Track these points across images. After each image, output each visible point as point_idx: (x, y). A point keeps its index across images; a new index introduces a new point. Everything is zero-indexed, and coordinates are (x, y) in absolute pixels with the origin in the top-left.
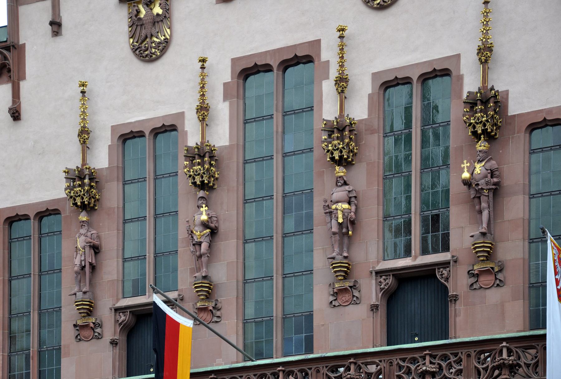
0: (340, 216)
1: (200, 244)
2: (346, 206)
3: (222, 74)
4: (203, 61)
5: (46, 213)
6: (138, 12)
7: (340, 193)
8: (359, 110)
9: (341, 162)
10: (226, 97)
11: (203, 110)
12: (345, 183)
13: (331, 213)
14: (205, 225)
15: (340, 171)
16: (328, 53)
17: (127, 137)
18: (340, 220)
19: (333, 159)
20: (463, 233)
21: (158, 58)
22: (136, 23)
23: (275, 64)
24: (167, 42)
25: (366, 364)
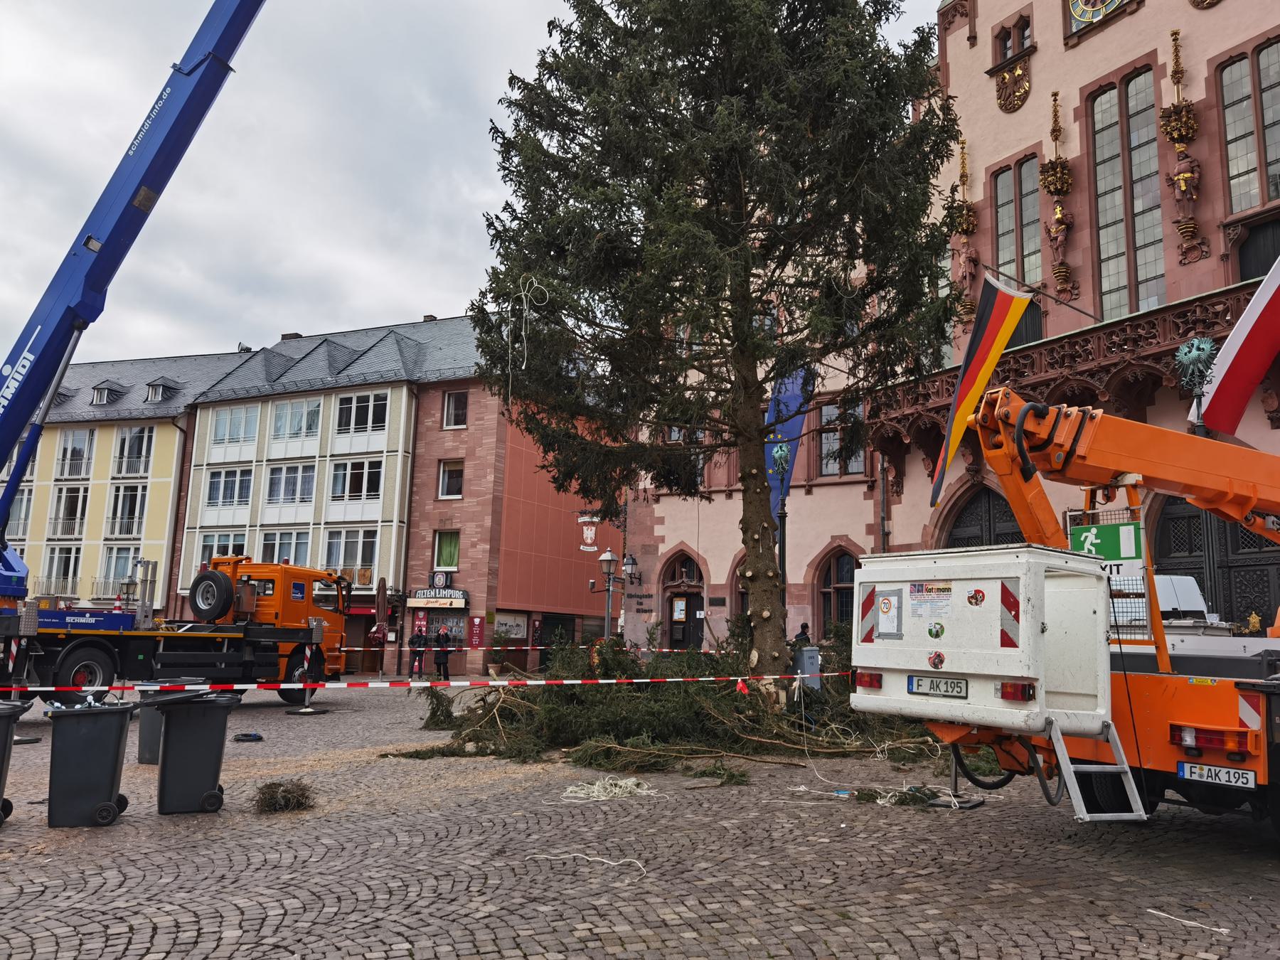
0: (1182, 184)
1: (1056, 239)
2: (1188, 175)
3: (1072, 100)
4: (1055, 94)
6: (1004, 78)
8: (1197, 93)
9: (1181, 139)
11: (1057, 133)
12: (1187, 156)
13: (1172, 183)
14: (1059, 222)
15: (1179, 147)
16: (1165, 58)
18: (1183, 188)
19: (1173, 139)
21: (1020, 107)
22: (1001, 88)
23: (1116, 80)
24: (1027, 93)
25: (1213, 305)
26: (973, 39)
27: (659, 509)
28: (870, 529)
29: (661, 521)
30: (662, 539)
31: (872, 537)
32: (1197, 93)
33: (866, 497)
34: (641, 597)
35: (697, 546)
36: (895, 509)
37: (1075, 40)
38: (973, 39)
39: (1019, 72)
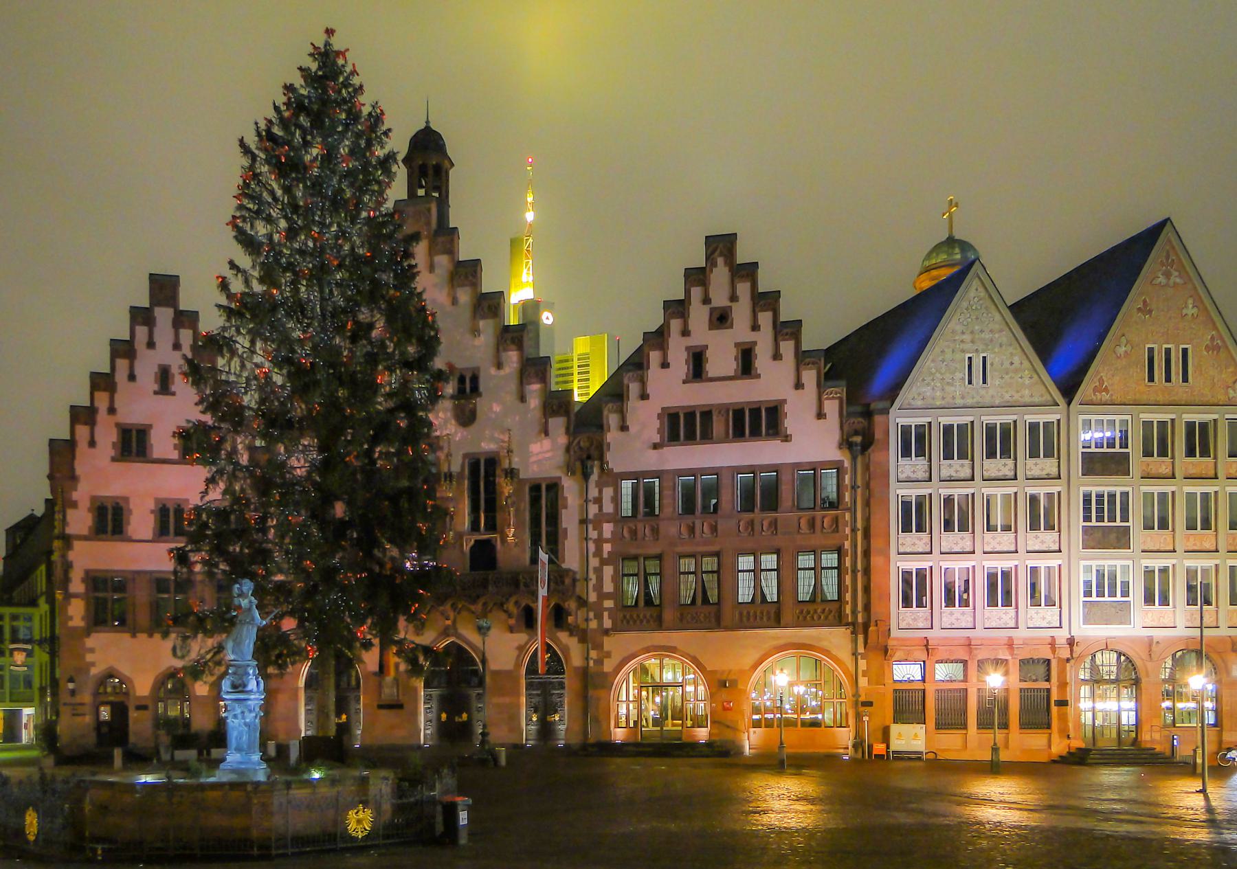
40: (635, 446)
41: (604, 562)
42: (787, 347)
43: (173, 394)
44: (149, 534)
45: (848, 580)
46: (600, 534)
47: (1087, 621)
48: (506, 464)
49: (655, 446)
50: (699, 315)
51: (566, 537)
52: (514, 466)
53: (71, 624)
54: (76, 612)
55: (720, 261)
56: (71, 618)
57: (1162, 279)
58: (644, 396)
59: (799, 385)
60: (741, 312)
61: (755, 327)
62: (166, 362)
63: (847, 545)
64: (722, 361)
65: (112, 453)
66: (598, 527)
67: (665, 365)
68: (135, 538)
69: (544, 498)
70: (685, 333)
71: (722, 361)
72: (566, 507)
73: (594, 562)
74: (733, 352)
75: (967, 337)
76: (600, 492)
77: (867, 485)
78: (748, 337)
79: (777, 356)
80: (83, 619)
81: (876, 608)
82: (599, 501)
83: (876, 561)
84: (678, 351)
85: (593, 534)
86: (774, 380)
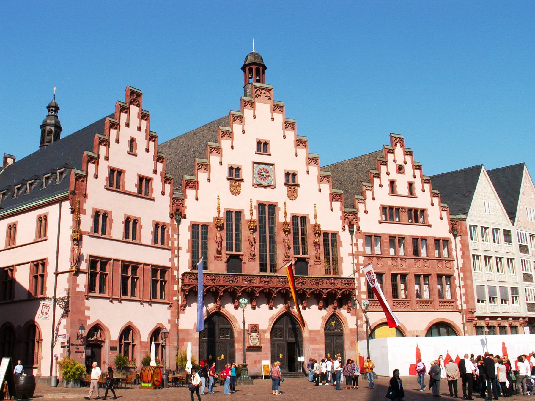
3: (255, 204)
5: (205, 226)
7: (286, 238)
10: (255, 209)
11: (251, 211)
17: (229, 213)
20: (312, 252)
26: (221, 164)
27: (88, 303)
28: (169, 321)
29: (88, 308)
30: (89, 318)
31: (170, 325)
32: (289, 220)
33: (169, 309)
34: (78, 345)
35: (105, 322)
36: (181, 315)
37: (256, 186)
38: (221, 164)
39: (237, 184)
40: (370, 221)
41: (361, 276)
42: (427, 186)
43: (136, 155)
44: (121, 237)
45: (457, 290)
46: (358, 261)
47: (529, 311)
48: (312, 221)
49: (380, 223)
50: (392, 167)
51: (343, 262)
52: (318, 223)
53: (78, 289)
54: (82, 280)
55: (399, 145)
56: (78, 286)
57: (525, 184)
58: (374, 199)
59: (432, 204)
60: (408, 168)
61: (414, 176)
62: (134, 136)
63: (456, 275)
64: (402, 188)
65: (105, 183)
66: (357, 258)
67: (381, 186)
68: (113, 238)
69: (330, 240)
70: (388, 174)
71: (402, 188)
72: (342, 247)
73: (357, 275)
74: (407, 185)
75: (483, 194)
76: (357, 241)
77: (461, 249)
78: (412, 180)
79: (423, 191)
80: (85, 286)
81: (471, 302)
82: (356, 245)
83: (469, 282)
84: (385, 180)
85: (356, 261)
86: (424, 199)
